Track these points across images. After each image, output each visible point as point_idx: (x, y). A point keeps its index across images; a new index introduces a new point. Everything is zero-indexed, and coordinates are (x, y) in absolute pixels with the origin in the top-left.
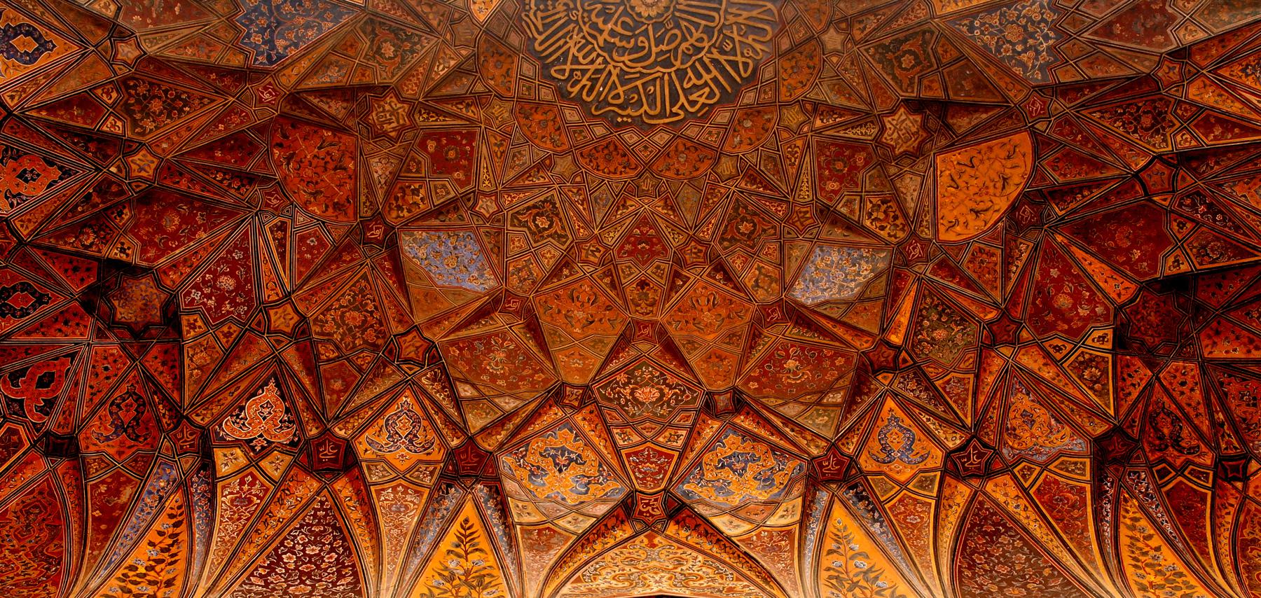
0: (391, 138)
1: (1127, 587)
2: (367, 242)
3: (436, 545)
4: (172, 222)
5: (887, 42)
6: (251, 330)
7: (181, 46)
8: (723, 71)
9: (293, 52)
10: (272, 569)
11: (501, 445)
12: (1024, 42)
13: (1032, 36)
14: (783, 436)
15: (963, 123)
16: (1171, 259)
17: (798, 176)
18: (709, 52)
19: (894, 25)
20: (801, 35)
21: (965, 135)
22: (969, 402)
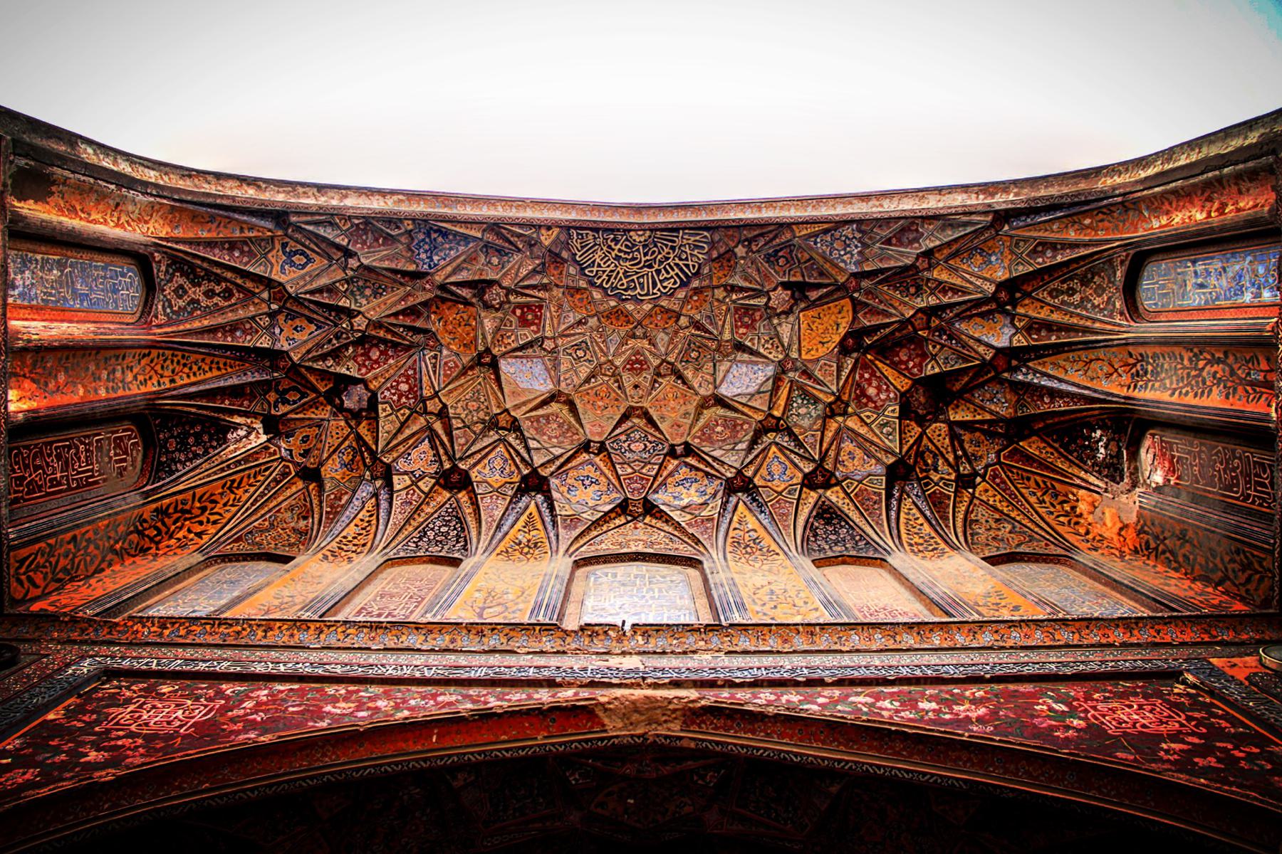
1: (902, 545)
2: (482, 365)
3: (512, 526)
4: (375, 354)
5: (770, 251)
6: (417, 412)
7: (381, 260)
8: (681, 270)
9: (442, 263)
10: (420, 538)
11: (552, 473)
12: (845, 249)
13: (849, 246)
14: (712, 467)
15: (814, 295)
16: (929, 366)
17: (723, 326)
19: (774, 243)
20: (722, 250)
21: (815, 301)
22: (818, 447)
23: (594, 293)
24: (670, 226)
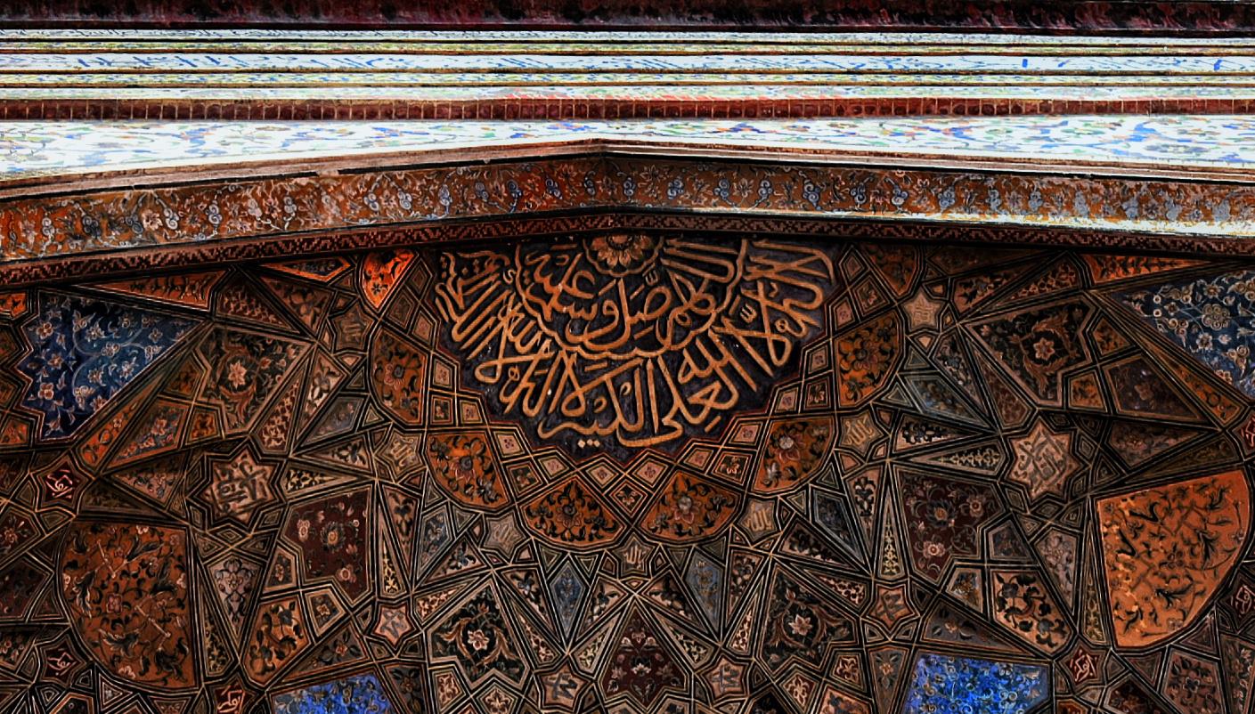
0: (240, 524)
8: (741, 354)
9: (101, 405)
12: (1232, 331)
15: (1137, 450)
17: (876, 538)
18: (718, 322)
23: (502, 438)
24: (712, 227)
